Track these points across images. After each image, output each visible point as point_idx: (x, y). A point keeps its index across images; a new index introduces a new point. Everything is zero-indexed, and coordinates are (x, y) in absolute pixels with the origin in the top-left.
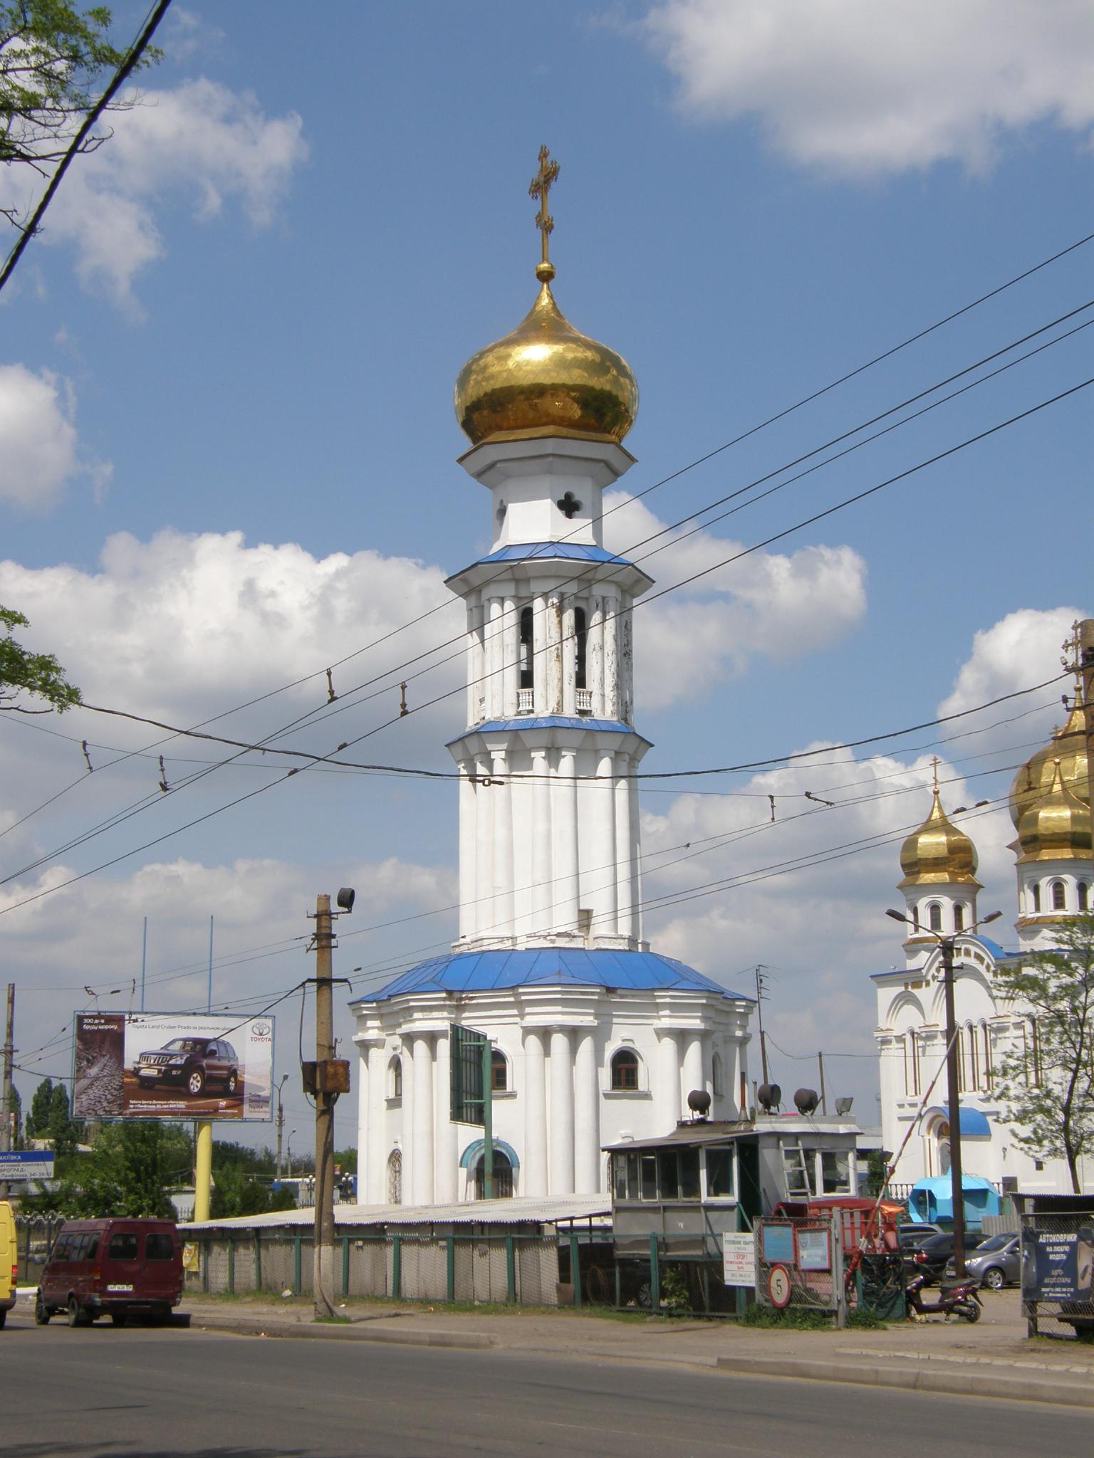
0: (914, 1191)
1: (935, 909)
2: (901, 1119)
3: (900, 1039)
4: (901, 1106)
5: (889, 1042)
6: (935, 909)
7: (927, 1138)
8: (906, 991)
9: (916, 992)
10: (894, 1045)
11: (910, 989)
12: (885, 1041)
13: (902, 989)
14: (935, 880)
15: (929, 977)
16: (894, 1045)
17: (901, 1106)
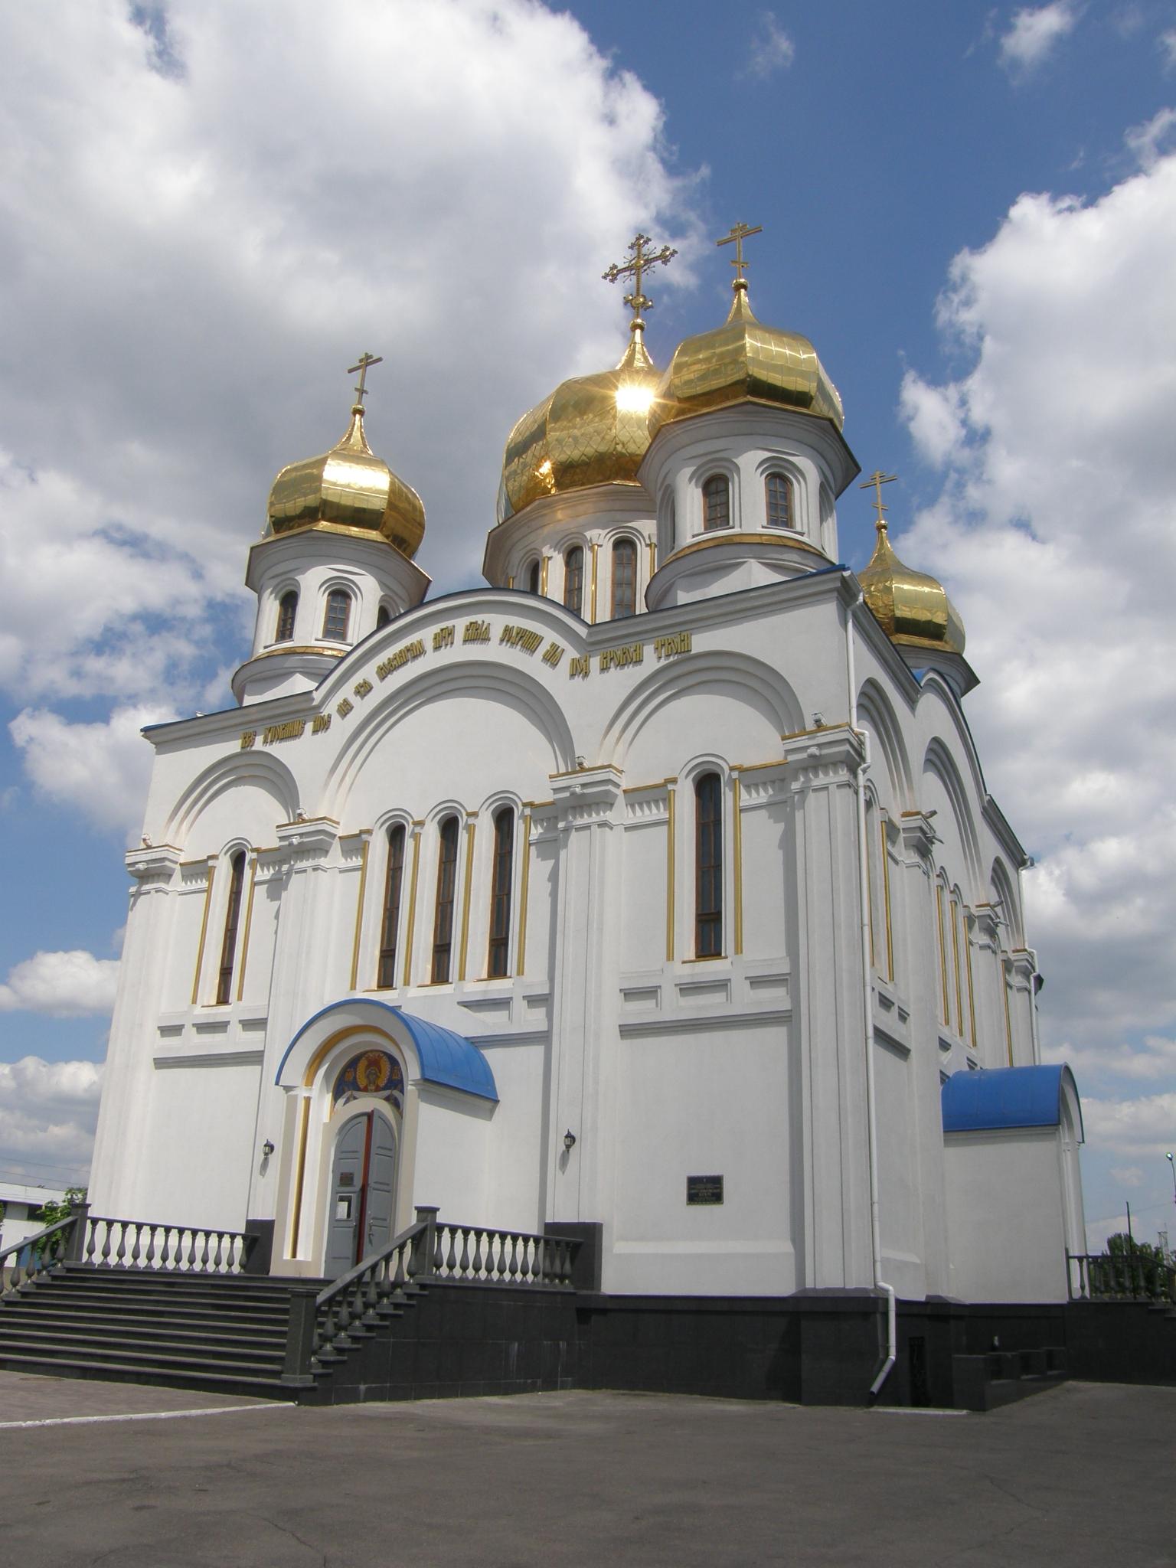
0: (1121, 1245)
1: (340, 595)
2: (161, 1063)
3: (200, 869)
4: (171, 1031)
5: (167, 876)
6: (340, 595)
7: (302, 1093)
8: (246, 751)
9: (280, 750)
10: (177, 884)
11: (258, 744)
12: (154, 873)
13: (234, 746)
14: (361, 535)
15: (331, 709)
16: (177, 884)
17: (171, 1031)
